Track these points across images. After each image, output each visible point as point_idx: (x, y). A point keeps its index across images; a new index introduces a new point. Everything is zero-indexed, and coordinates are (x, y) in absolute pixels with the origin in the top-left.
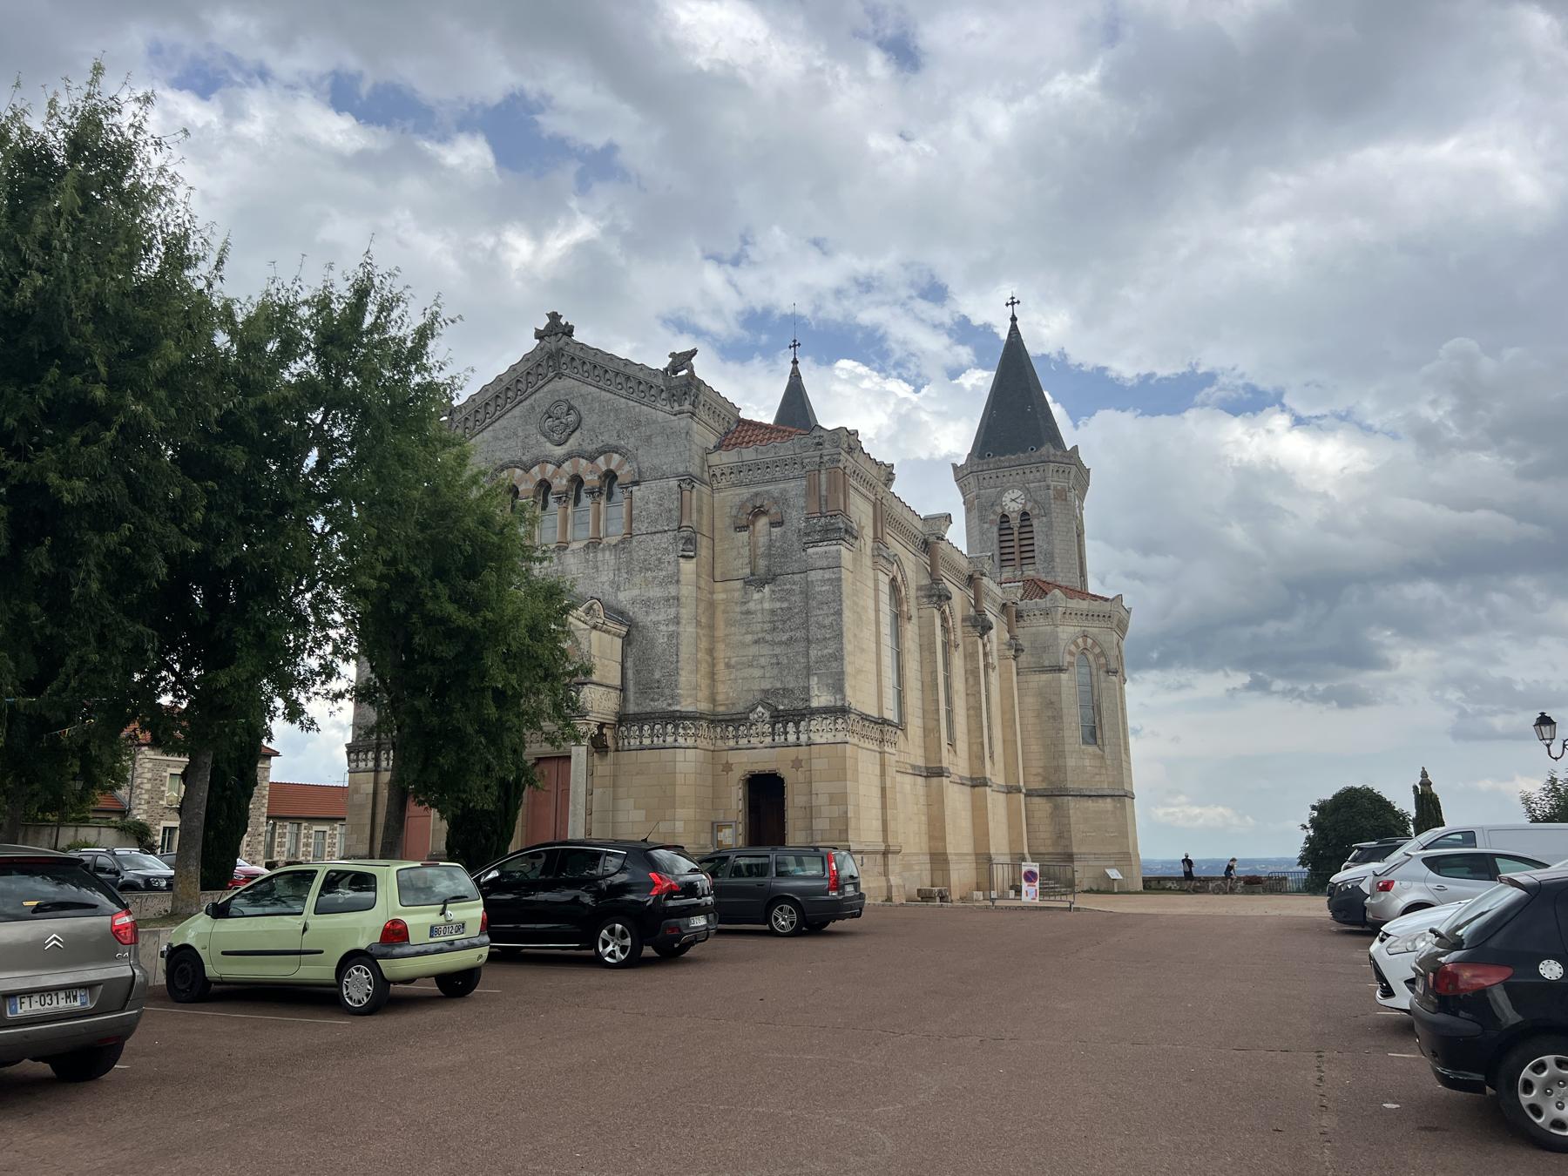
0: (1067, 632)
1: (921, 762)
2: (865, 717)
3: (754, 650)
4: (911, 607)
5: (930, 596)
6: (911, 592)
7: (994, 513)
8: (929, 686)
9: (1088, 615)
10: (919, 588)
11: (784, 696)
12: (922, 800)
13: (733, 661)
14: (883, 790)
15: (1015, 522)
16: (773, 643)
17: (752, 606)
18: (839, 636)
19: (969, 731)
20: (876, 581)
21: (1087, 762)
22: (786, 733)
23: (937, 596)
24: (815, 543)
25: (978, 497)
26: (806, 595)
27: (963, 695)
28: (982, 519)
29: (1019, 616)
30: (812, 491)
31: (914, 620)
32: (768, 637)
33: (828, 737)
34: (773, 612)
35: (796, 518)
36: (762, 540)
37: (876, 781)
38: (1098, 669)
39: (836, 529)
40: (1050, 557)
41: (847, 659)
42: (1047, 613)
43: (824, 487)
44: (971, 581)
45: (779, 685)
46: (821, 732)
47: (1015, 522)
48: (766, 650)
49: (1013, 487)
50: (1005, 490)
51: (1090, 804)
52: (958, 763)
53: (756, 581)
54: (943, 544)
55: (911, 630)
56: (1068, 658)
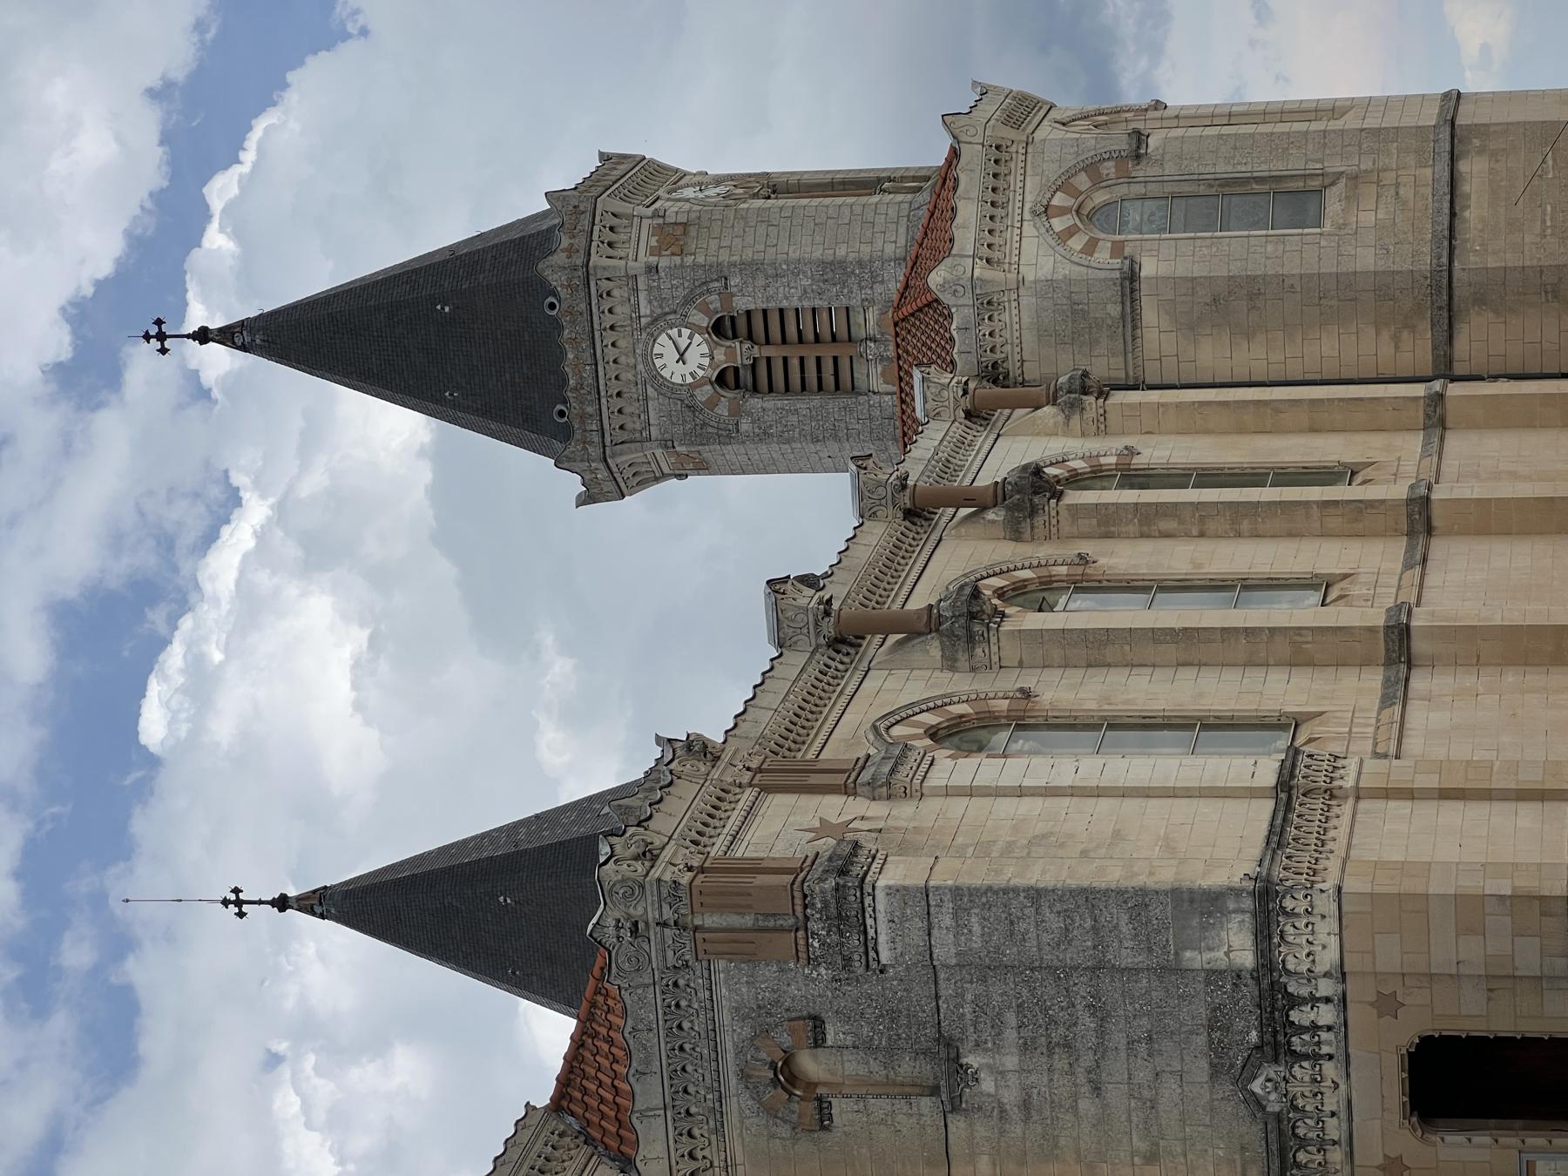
0: (1038, 256)
1: (1374, 680)
2: (1276, 838)
3: (1115, 1094)
4: (997, 689)
5: (971, 639)
6: (962, 688)
7: (712, 403)
8: (1190, 647)
9: (995, 200)
10: (950, 664)
11: (1227, 1029)
12: (1468, 680)
13: (1141, 1145)
14: (1445, 794)
15: (740, 353)
16: (1101, 1050)
17: (1010, 1097)
18: (1089, 897)
19: (1291, 535)
20: (949, 792)
21: (1368, 218)
22: (1314, 1028)
23: (966, 621)
24: (869, 946)
25: (667, 444)
26: (985, 969)
27: (1205, 546)
28: (728, 435)
29: (994, 374)
30: (742, 947)
31: (1029, 680)
32: (1087, 1060)
33: (1326, 931)
34: (1026, 1047)
35: (806, 987)
36: (853, 1066)
37: (1426, 809)
38: (1131, 180)
39: (833, 898)
40: (833, 271)
41: (1142, 880)
42: (987, 305)
43: (734, 920)
44: (918, 512)
45: (1201, 1040)
46: (1314, 947)
47: (740, 353)
48: (1116, 1067)
49: (648, 358)
50: (655, 377)
51: (1473, 215)
52: (1373, 569)
53: (950, 1084)
54: (836, 591)
55: (1060, 690)
56: (1103, 256)
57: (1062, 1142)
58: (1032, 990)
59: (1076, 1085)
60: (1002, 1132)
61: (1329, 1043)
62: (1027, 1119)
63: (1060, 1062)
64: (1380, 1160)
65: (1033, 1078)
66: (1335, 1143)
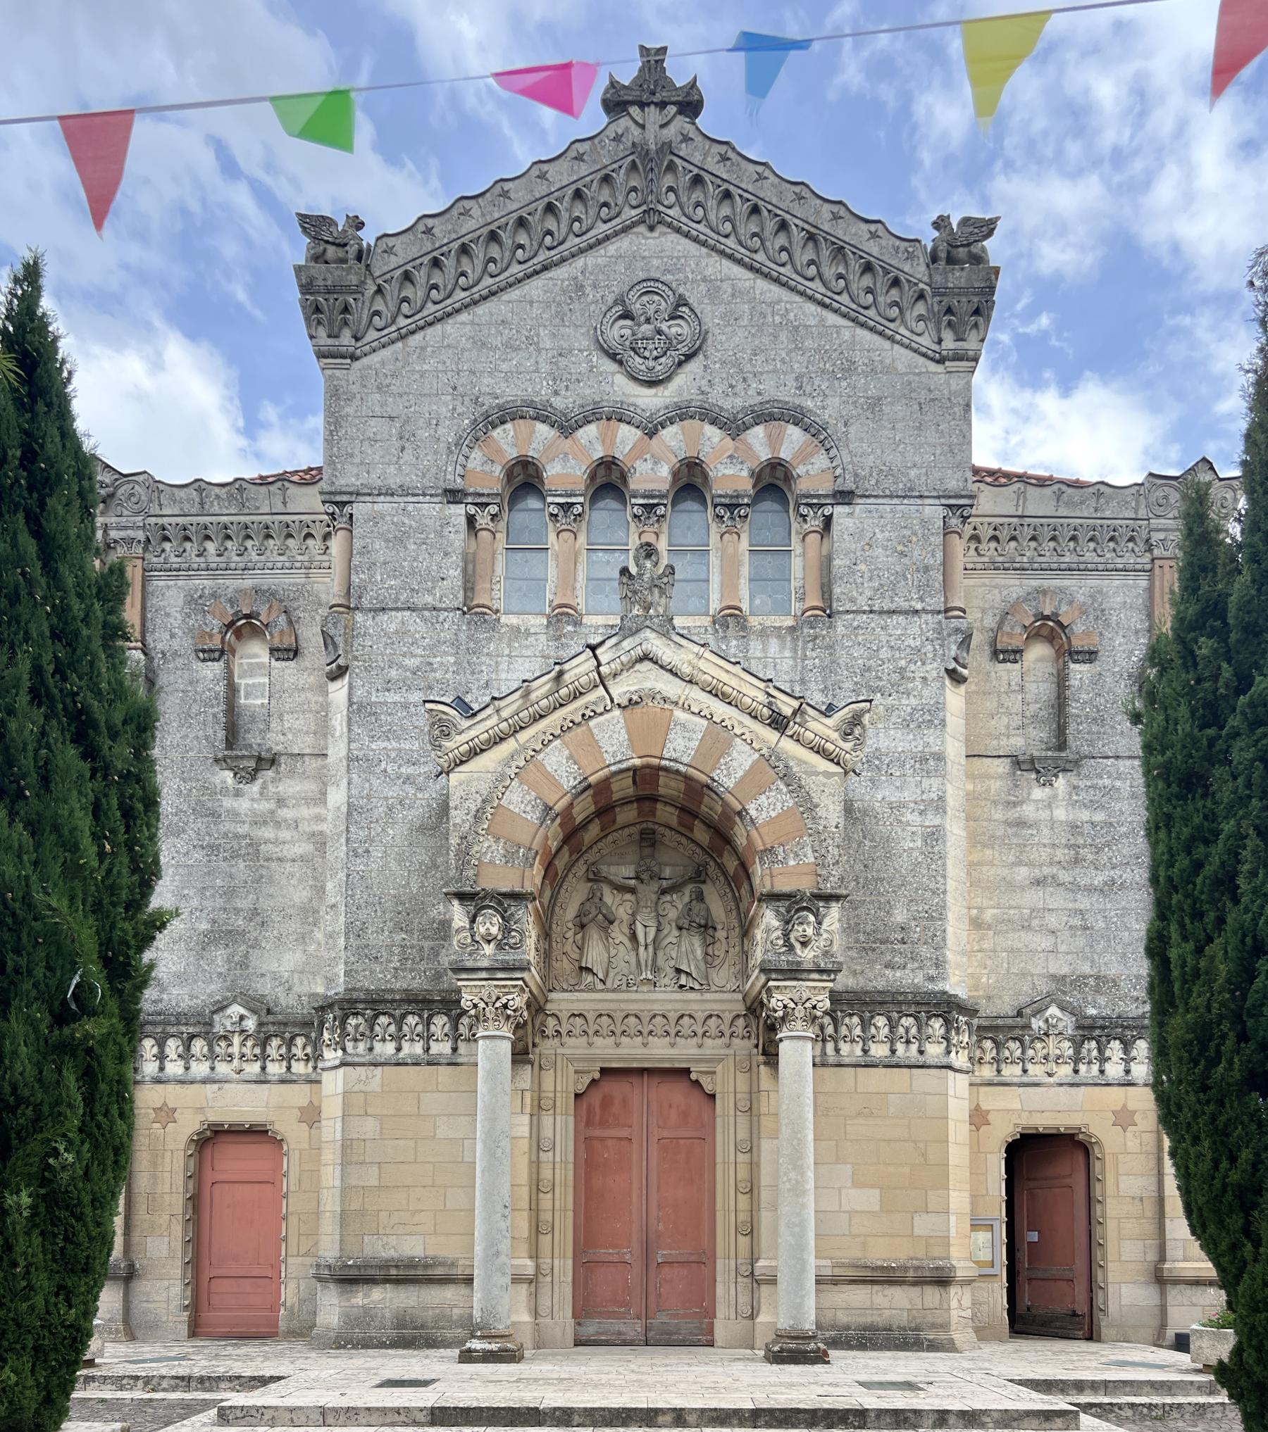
13: (988, 915)
17: (1028, 811)
34: (1074, 828)
57: (988, 852)
58: (1126, 835)
59: (1041, 865)
60: (994, 802)
61: (1088, 1071)
62: (1009, 824)
63: (1060, 854)
64: (984, 1107)
65: (1046, 831)
66: (999, 1071)
